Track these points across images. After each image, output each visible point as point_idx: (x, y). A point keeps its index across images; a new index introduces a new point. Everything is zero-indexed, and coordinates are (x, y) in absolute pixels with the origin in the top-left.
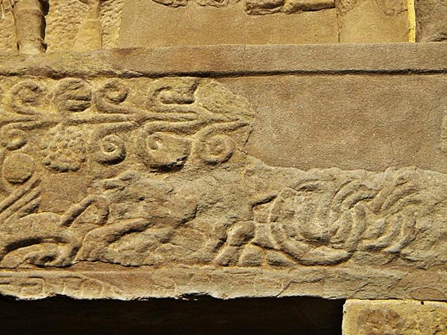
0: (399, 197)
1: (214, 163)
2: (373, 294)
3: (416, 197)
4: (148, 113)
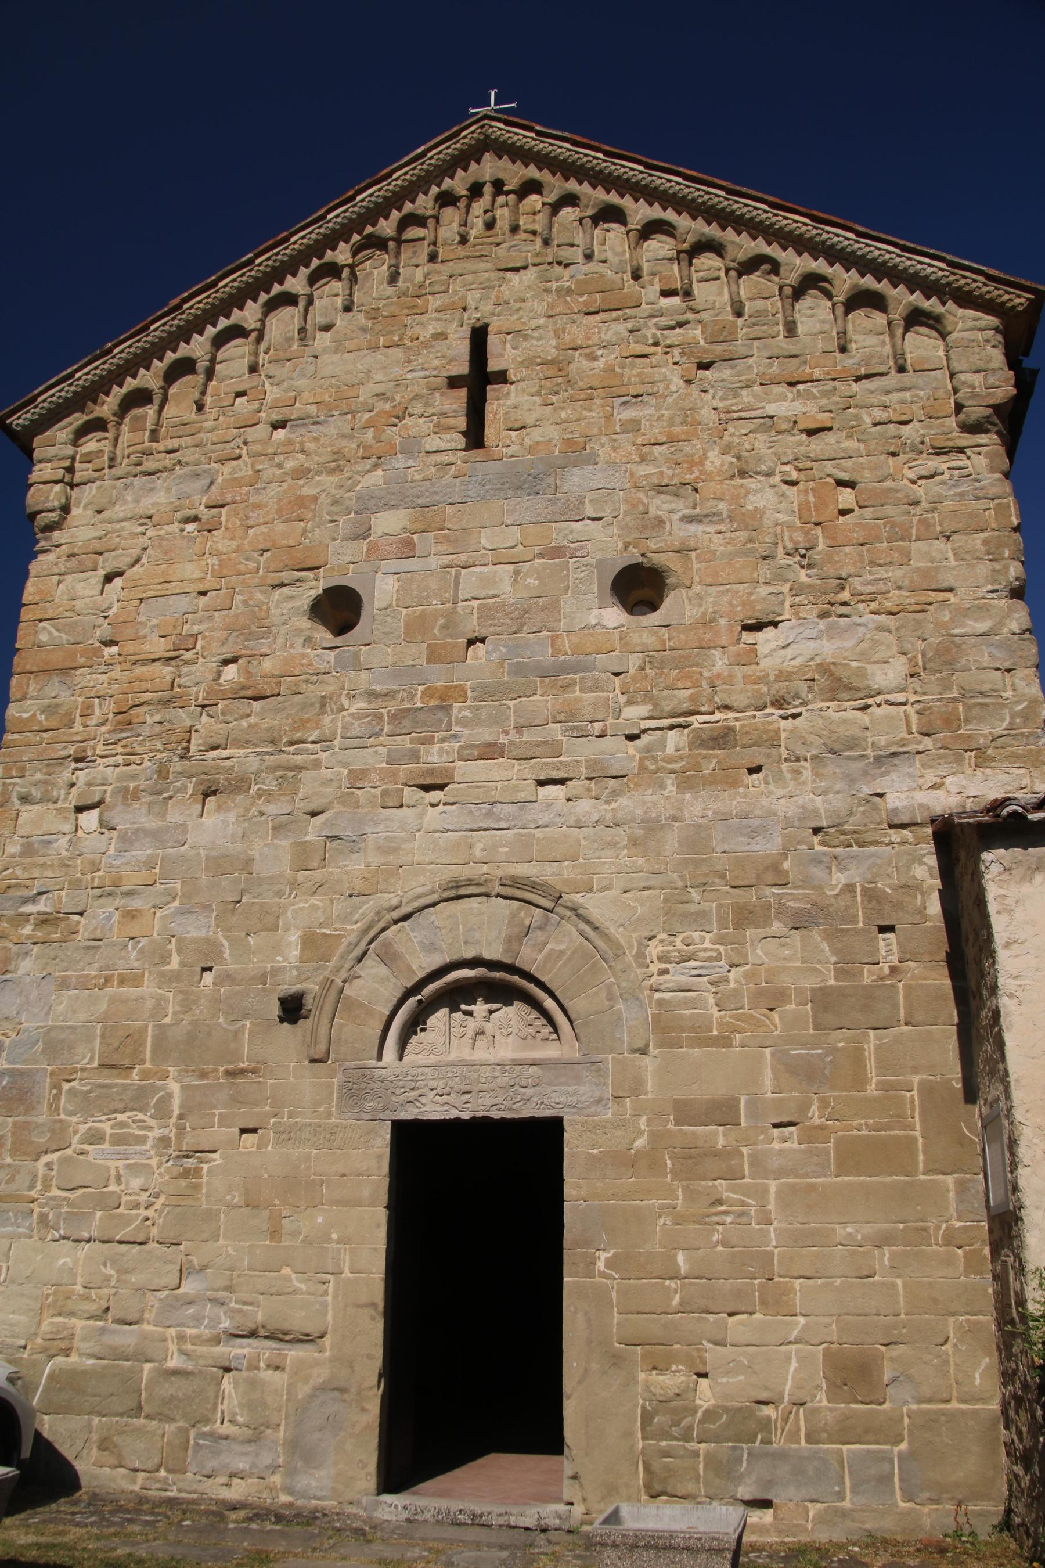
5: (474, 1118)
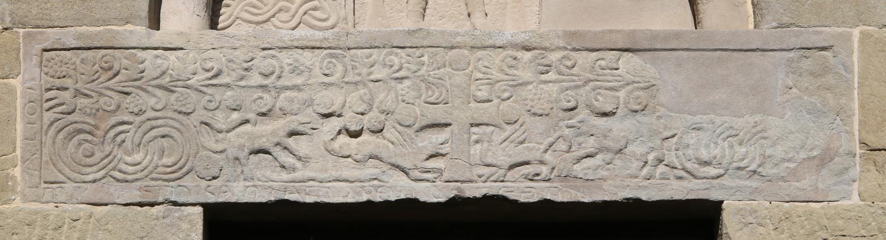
0: (755, 135)
1: (636, 111)
2: (740, 198)
3: (766, 135)
4: (591, 77)
5: (457, 203)
